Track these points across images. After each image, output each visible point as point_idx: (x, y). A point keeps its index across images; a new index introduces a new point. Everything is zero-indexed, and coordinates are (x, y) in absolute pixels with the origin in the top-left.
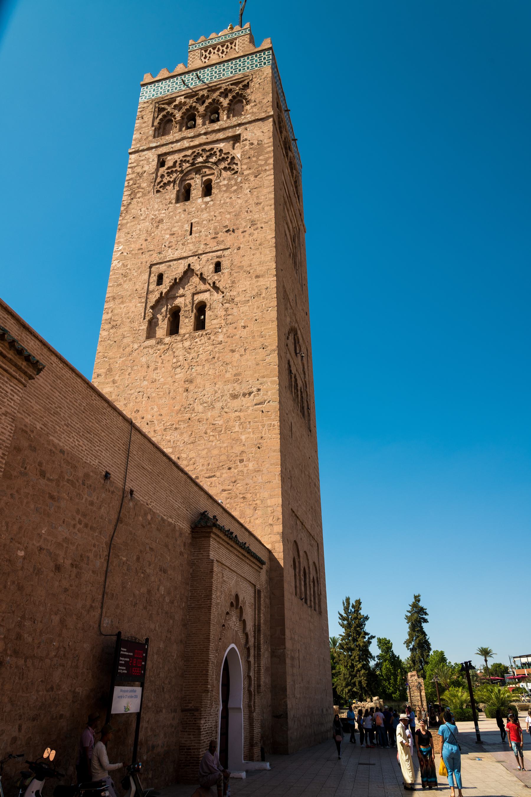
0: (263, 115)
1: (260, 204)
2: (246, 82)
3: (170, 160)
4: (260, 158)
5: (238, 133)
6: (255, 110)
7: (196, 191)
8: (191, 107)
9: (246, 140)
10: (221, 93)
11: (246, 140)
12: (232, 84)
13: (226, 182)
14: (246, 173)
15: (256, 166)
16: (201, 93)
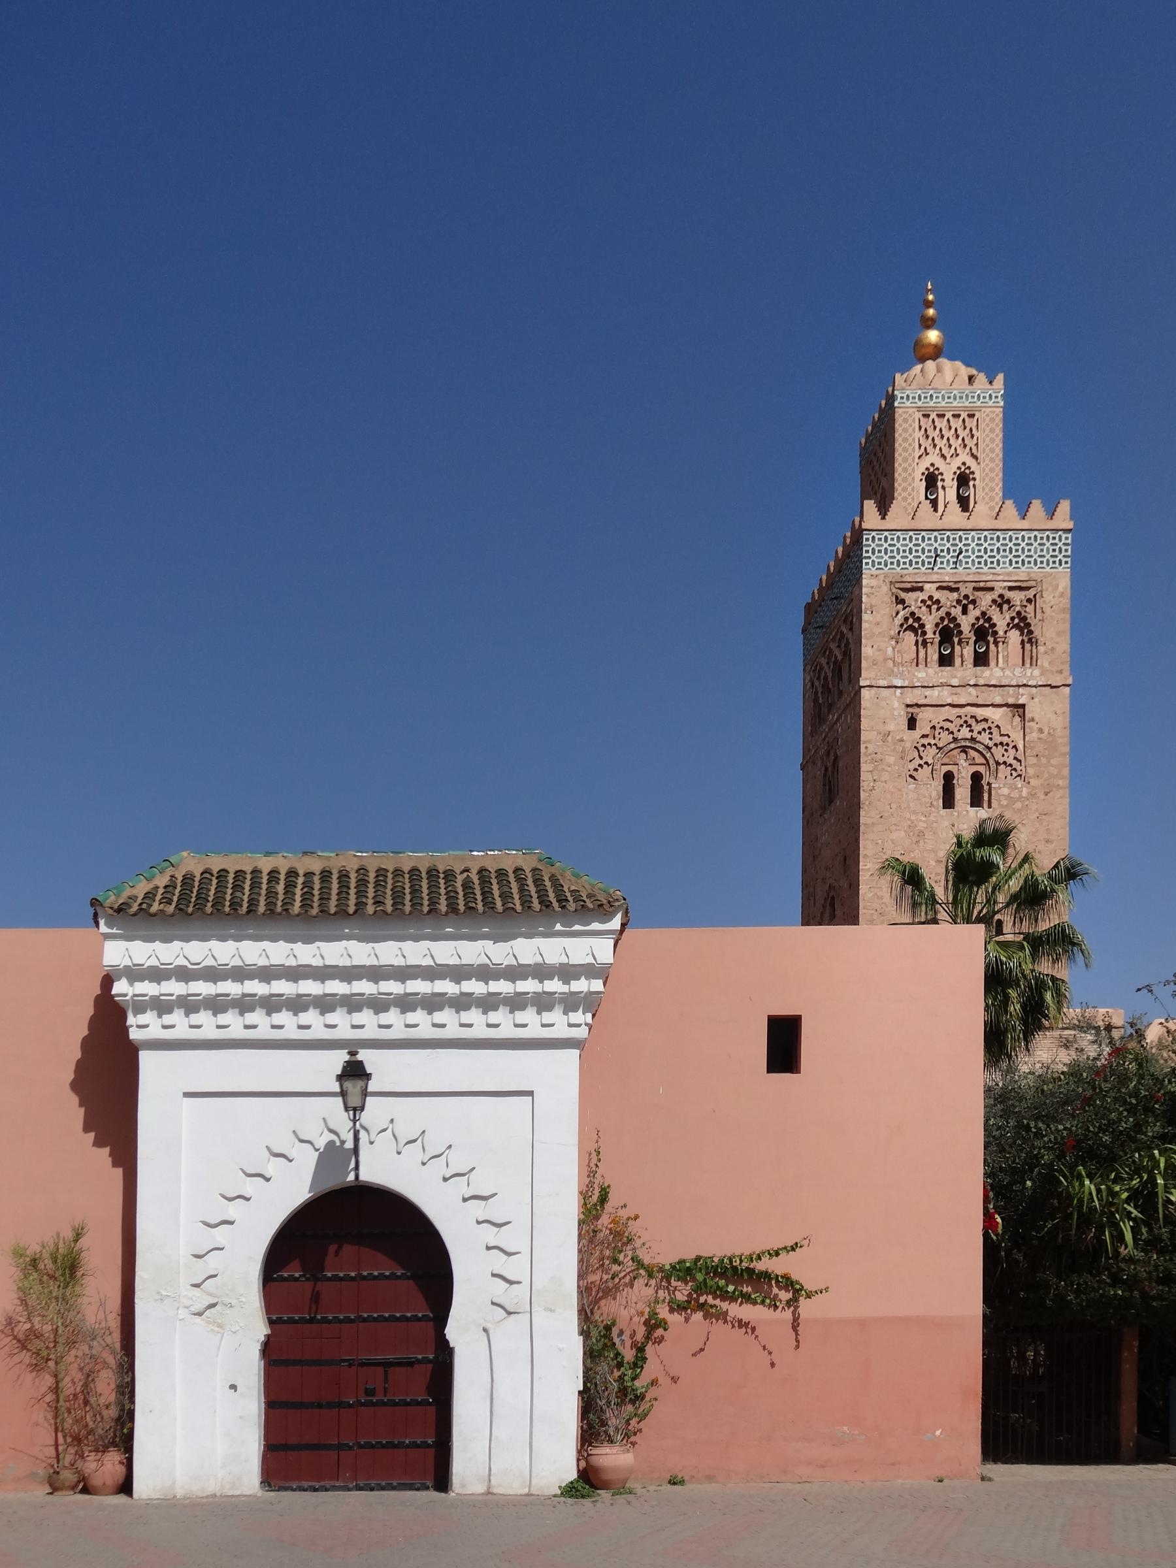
0: (1057, 680)
1: (1052, 842)
2: (1030, 594)
3: (926, 717)
4: (1053, 761)
5: (1021, 702)
6: (1046, 664)
7: (962, 792)
8: (948, 614)
9: (1033, 720)
10: (994, 601)
11: (1033, 720)
12: (1010, 589)
13: (1005, 791)
14: (1033, 782)
15: (1046, 776)
16: (964, 591)
